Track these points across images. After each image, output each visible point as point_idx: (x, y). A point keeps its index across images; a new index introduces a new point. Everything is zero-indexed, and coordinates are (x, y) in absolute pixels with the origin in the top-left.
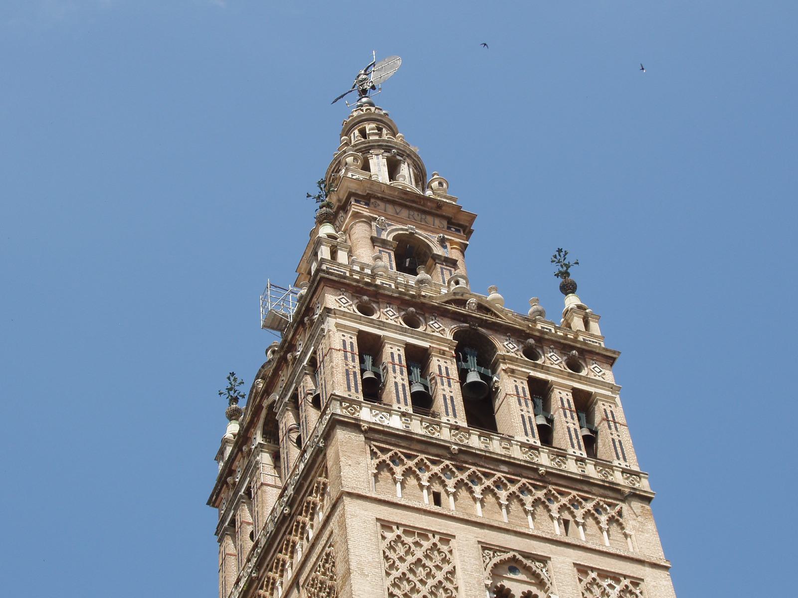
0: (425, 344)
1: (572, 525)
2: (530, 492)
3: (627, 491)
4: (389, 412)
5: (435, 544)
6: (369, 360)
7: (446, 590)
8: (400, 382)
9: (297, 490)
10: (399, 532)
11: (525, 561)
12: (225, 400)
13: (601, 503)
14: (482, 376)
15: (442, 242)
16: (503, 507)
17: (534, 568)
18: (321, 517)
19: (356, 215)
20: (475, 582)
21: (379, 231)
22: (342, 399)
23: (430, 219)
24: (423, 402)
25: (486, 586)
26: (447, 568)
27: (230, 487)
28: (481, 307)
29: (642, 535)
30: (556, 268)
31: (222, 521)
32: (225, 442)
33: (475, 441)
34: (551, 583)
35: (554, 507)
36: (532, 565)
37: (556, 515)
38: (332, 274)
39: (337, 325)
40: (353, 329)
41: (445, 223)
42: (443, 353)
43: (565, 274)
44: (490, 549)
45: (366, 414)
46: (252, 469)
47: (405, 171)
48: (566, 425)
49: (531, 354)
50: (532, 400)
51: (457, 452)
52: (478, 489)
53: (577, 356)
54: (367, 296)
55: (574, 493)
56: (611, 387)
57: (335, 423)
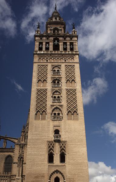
0: (48, 41)
26: (46, 69)
28: (57, 34)
33: (53, 52)
49: (65, 39)
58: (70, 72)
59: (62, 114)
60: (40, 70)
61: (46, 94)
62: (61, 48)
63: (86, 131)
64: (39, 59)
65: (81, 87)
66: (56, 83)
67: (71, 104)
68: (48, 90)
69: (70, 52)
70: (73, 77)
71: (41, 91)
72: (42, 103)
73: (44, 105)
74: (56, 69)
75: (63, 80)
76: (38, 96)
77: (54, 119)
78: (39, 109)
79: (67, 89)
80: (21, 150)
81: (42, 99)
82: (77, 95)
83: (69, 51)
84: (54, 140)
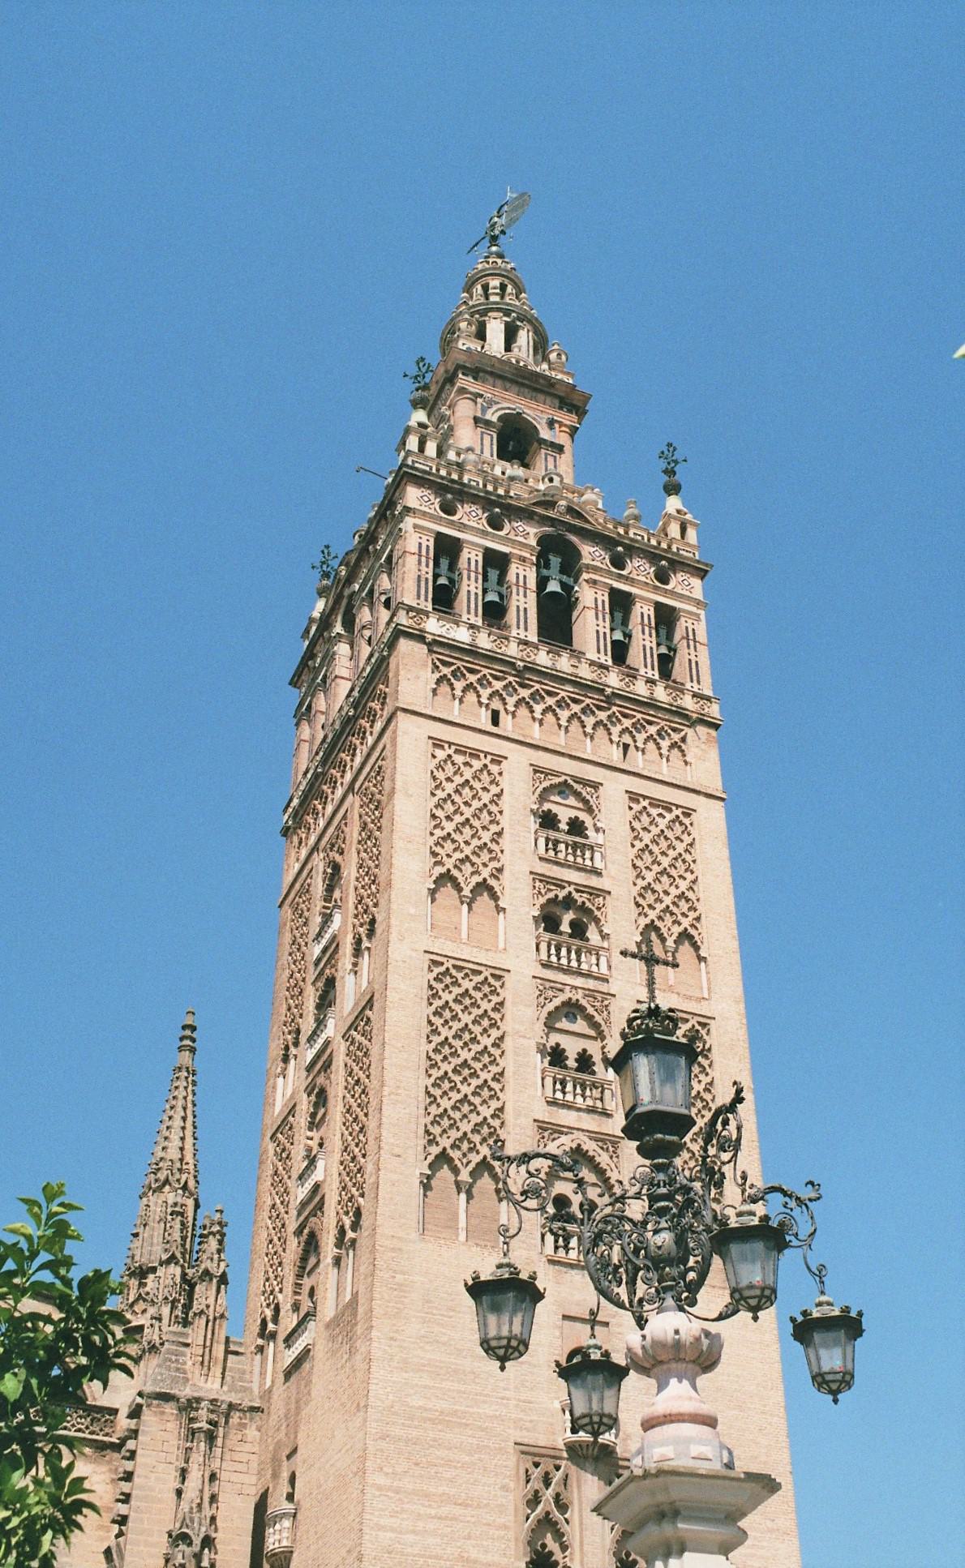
1: (632, 749)
2: (593, 713)
3: (695, 716)
4: (457, 623)
5: (485, 766)
6: (444, 563)
7: (490, 813)
8: (473, 590)
9: (363, 693)
10: (451, 752)
11: (576, 786)
12: (317, 574)
14: (563, 585)
15: (551, 424)
18: (378, 726)
19: (462, 391)
21: (484, 410)
22: (410, 609)
23: (541, 397)
24: (495, 613)
26: (494, 790)
27: (309, 672)
28: (570, 510)
29: (703, 763)
30: (663, 464)
31: (301, 705)
32: (311, 620)
33: (543, 658)
35: (616, 730)
37: (615, 738)
38: (417, 469)
39: (415, 526)
40: (428, 530)
41: (557, 402)
42: (523, 560)
43: (670, 472)
45: (433, 626)
46: (329, 658)
47: (524, 337)
48: (643, 643)
49: (618, 562)
50: (611, 614)
53: (666, 566)
54: (452, 494)
55: (639, 716)
56: (698, 603)
57: (399, 633)
58: (665, 862)
61: (496, 1016)
62: (590, 626)
63: (787, 1395)
64: (438, 682)
65: (742, 1006)
66: (565, 927)
69: (661, 693)
71: (459, 975)
75: (620, 924)
80: (197, 1458)
83: (651, 682)
84: (571, 1448)
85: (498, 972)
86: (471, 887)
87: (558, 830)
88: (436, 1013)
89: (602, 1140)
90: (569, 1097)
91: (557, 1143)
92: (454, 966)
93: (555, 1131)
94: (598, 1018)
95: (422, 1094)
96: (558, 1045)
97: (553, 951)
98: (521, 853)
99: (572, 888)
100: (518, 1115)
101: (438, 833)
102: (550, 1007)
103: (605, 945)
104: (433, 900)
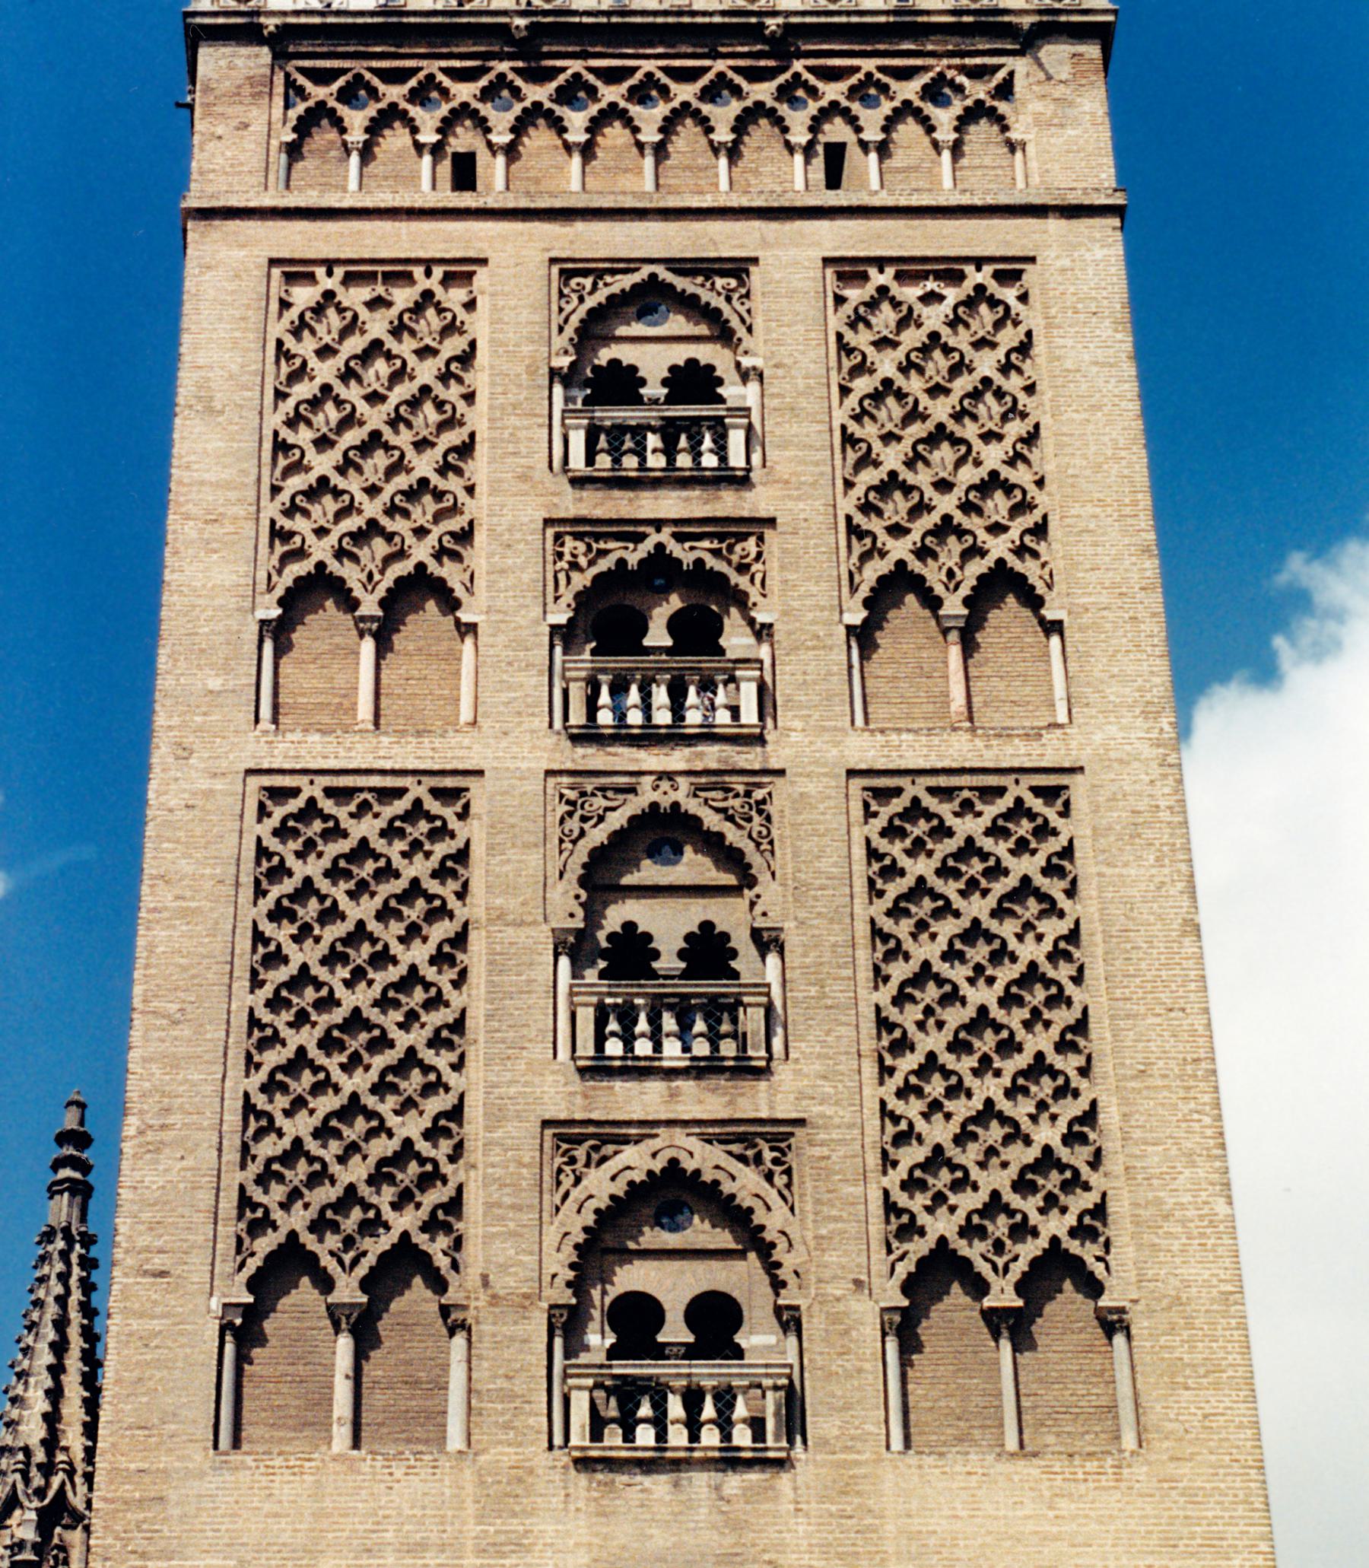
1: (853, 152)
2: (737, 92)
7: (439, 405)
10: (329, 284)
11: (681, 283)
13: (950, 74)
16: (648, 151)
17: (705, 296)
20: (521, 369)
25: (553, 373)
26: (454, 346)
34: (750, 330)
36: (699, 291)
44: (584, 273)
51: (524, 33)
52: (577, 121)
55: (869, 65)
58: (940, 410)
59: (790, 1321)
60: (325, 371)
61: (447, 890)
66: (658, 636)
67: (962, 1109)
68: (478, 793)
70: (998, 505)
71: (342, 813)
72: (359, 1082)
73: (412, 1127)
74: (652, 353)
75: (802, 588)
76: (282, 934)
77: (613, 1437)
78: (298, 1219)
79: (878, 786)
81: (361, 997)
82: (1085, 909)
85: (449, 782)
86: (381, 592)
87: (638, 400)
88: (278, 914)
89: (740, 1138)
90: (644, 1048)
91: (611, 1166)
92: (329, 792)
93: (606, 1140)
94: (734, 836)
95: (233, 1118)
96: (629, 926)
97: (605, 698)
98: (520, 485)
99: (665, 536)
100: (496, 1117)
101: (297, 482)
102: (598, 836)
103: (764, 652)
104: (279, 653)
